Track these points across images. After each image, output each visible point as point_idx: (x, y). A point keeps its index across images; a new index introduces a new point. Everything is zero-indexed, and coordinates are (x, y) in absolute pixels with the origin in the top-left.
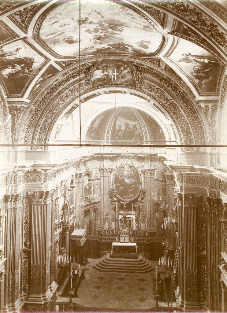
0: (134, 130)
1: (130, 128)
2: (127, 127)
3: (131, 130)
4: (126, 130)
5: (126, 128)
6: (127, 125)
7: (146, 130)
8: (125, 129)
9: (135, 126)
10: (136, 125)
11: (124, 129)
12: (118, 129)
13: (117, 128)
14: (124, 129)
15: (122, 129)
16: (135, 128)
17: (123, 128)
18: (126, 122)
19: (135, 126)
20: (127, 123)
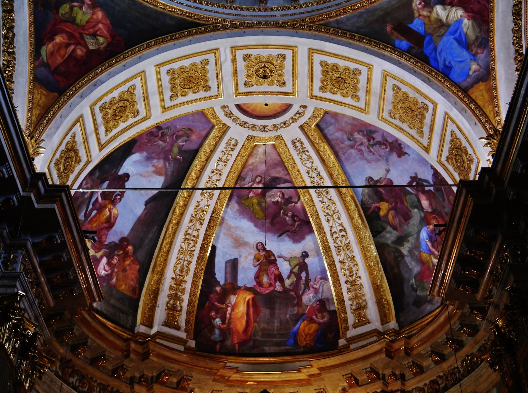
0: (296, 286)
1: (279, 278)
2: (266, 270)
3: (283, 284)
4: (258, 289)
5: (257, 277)
6: (266, 260)
7: (353, 258)
8: (255, 283)
9: (301, 265)
10: (305, 255)
11: (252, 283)
12: (222, 282)
13: (220, 275)
14: (252, 283)
15: (240, 284)
16: (303, 275)
17: (247, 275)
18: (261, 247)
19: (301, 265)
20: (265, 249)
